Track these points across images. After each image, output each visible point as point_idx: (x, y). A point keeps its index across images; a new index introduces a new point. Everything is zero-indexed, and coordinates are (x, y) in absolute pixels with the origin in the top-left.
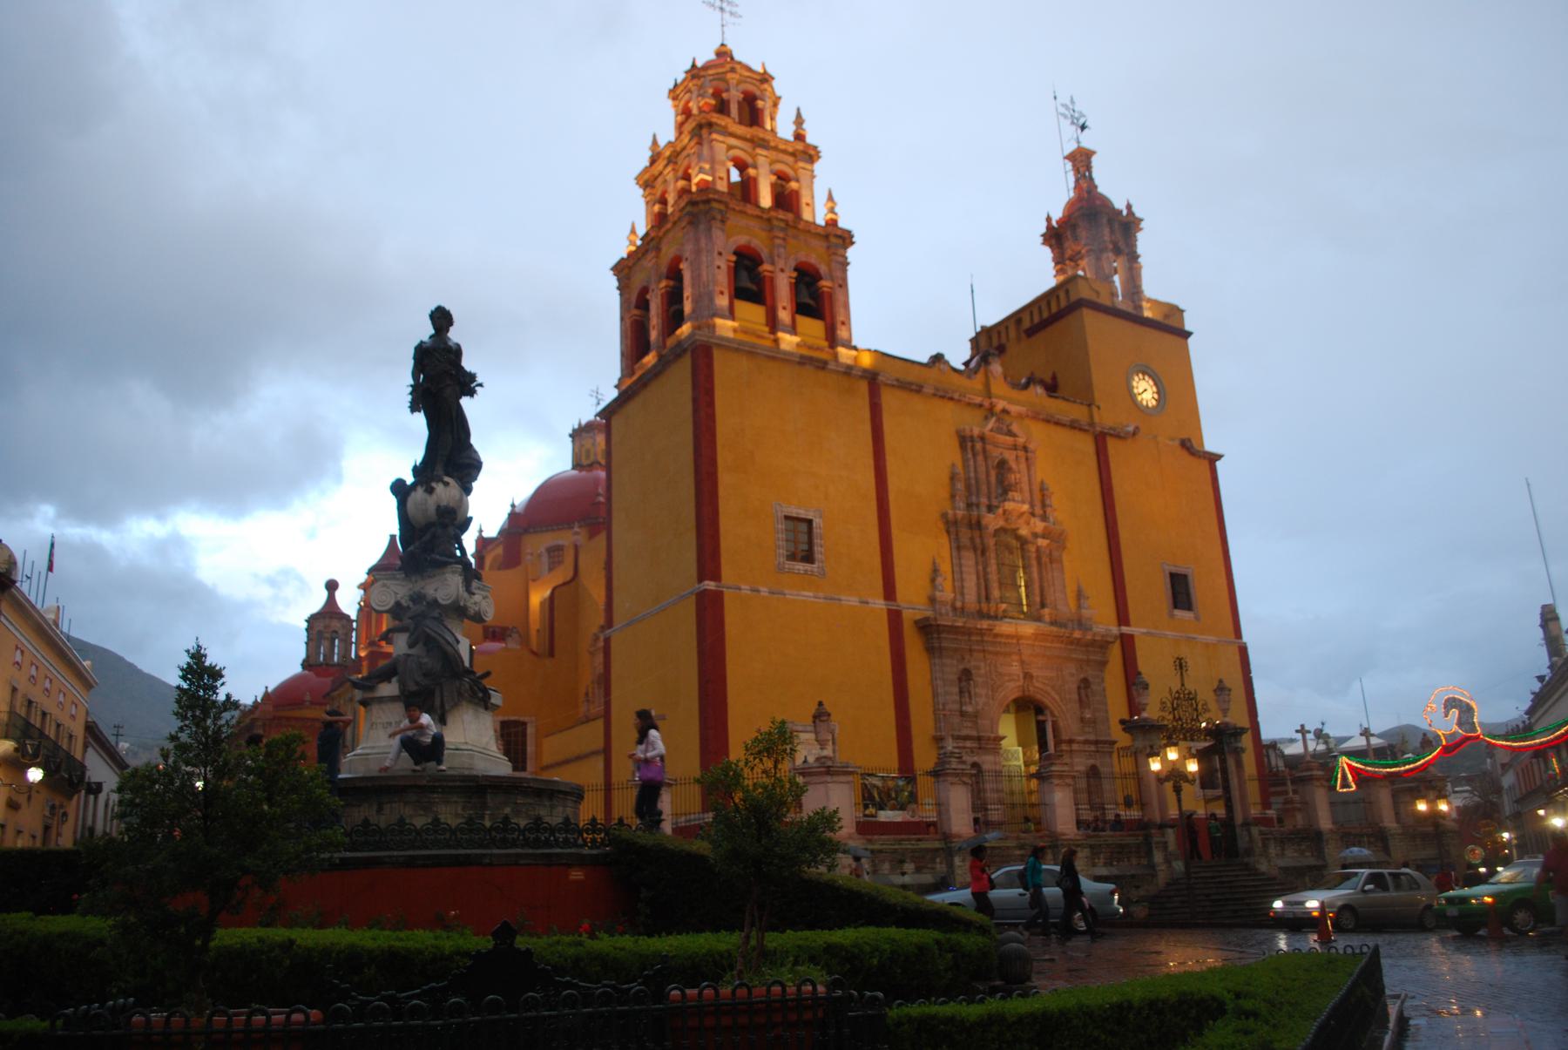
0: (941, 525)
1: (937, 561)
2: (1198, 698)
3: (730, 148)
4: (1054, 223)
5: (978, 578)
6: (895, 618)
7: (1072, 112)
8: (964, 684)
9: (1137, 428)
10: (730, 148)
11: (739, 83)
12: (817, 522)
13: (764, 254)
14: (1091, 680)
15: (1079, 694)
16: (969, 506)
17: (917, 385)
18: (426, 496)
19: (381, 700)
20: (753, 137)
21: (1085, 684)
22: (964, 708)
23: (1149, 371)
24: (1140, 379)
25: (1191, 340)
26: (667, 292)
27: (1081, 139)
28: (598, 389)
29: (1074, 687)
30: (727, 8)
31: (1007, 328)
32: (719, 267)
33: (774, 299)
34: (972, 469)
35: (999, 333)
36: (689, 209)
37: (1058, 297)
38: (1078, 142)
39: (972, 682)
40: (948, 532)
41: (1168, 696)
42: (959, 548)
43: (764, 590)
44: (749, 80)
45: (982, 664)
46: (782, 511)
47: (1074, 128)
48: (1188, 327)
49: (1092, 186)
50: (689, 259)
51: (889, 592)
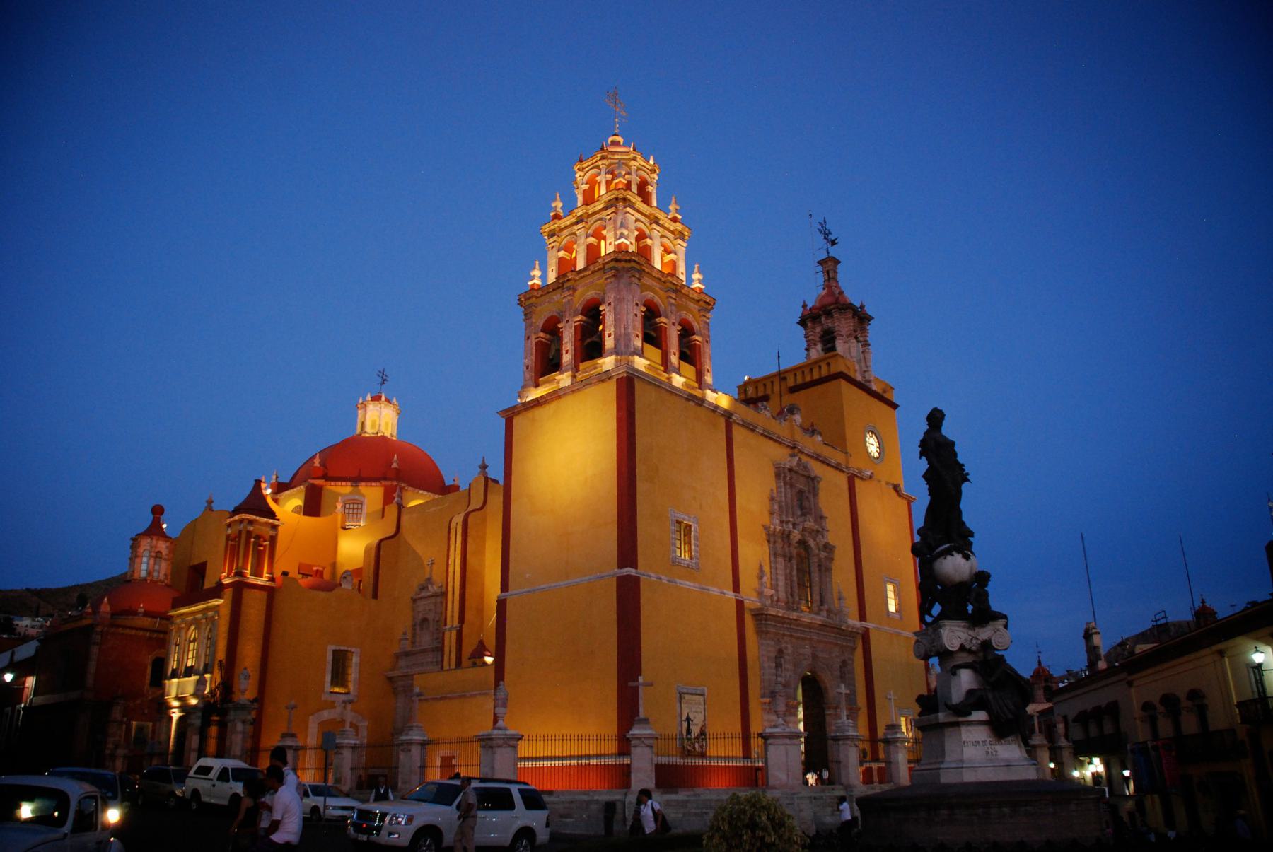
1: (763, 564)
3: (637, 220)
4: (808, 308)
5: (786, 579)
6: (740, 604)
9: (872, 473)
10: (637, 220)
11: (639, 169)
13: (662, 308)
16: (782, 522)
17: (754, 426)
18: (963, 561)
19: (970, 723)
20: (650, 214)
21: (844, 663)
23: (875, 431)
26: (582, 326)
27: (830, 251)
28: (384, 371)
29: (838, 666)
32: (636, 315)
34: (783, 495)
35: (765, 385)
36: (613, 264)
37: (820, 367)
38: (828, 253)
40: (769, 541)
42: (775, 555)
44: (643, 168)
45: (789, 646)
46: (675, 517)
47: (825, 241)
48: (895, 400)
50: (612, 304)
51: (736, 588)
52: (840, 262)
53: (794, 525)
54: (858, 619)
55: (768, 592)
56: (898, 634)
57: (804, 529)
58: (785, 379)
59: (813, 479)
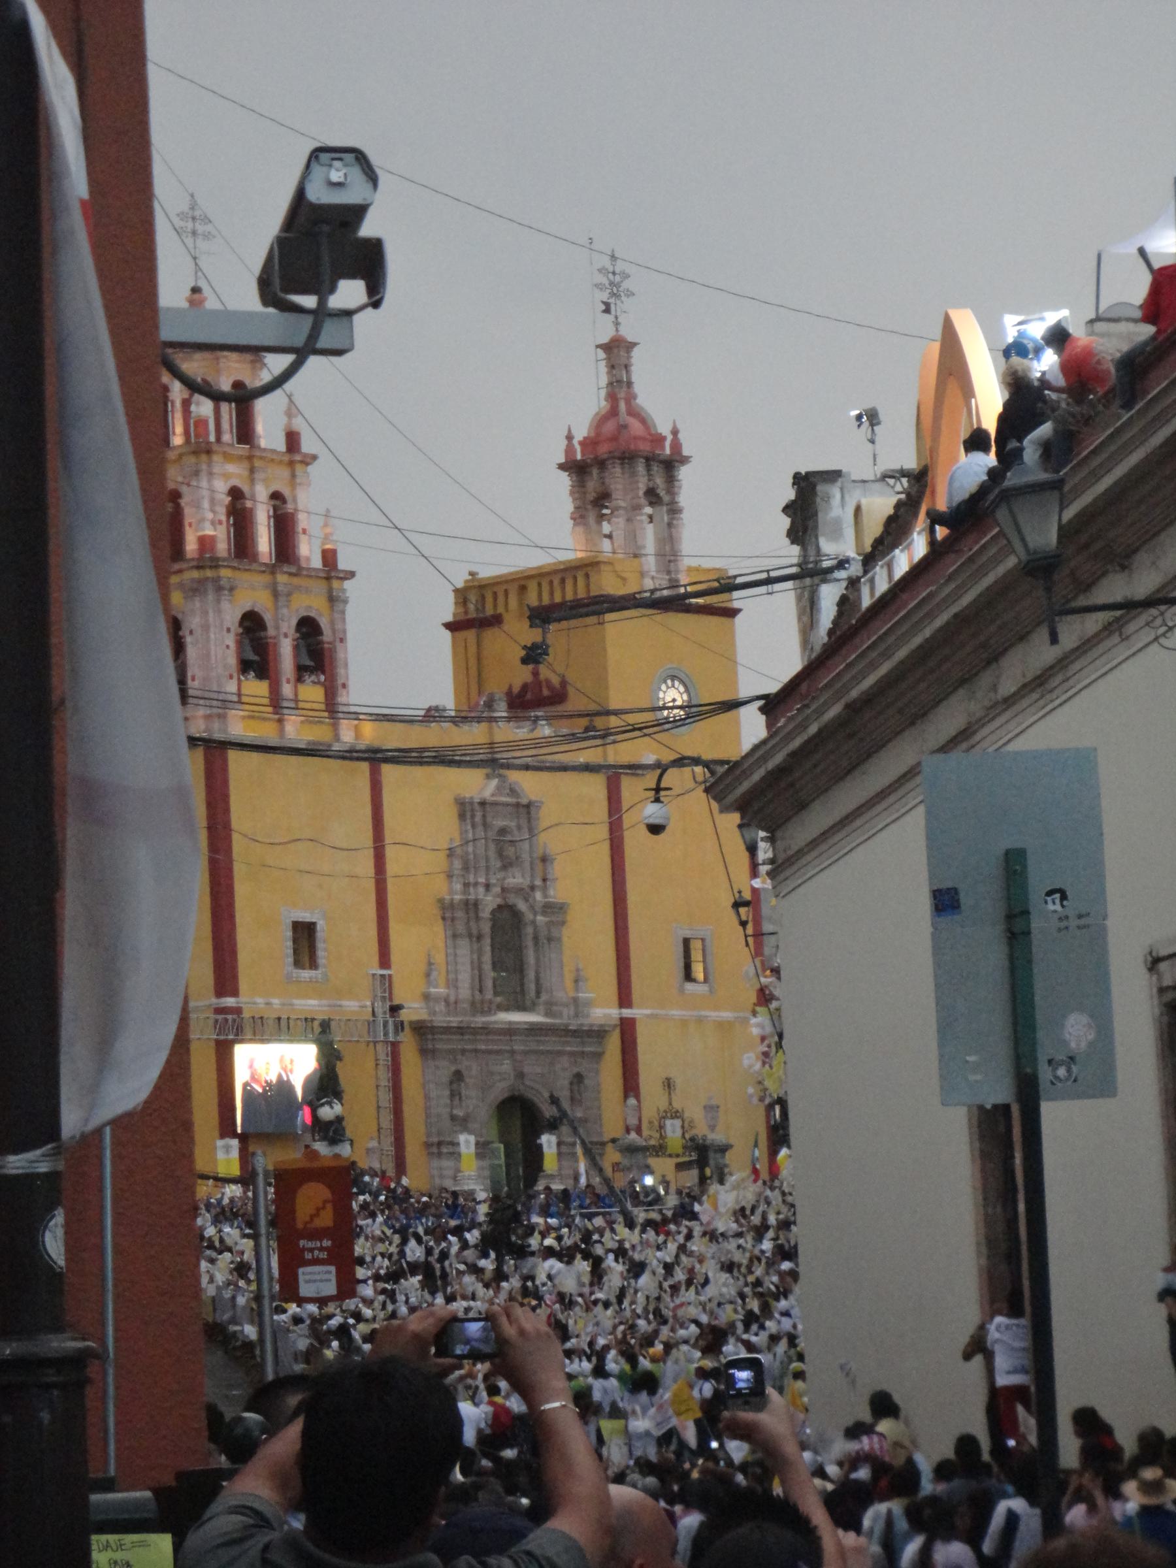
0: (436, 912)
2: (686, 1115)
5: (473, 969)
7: (611, 276)
8: (455, 1086)
12: (321, 925)
13: (268, 617)
14: (584, 1074)
15: (572, 1091)
16: (466, 885)
21: (579, 1077)
22: (455, 1112)
23: (682, 676)
24: (668, 687)
25: (739, 619)
29: (566, 1083)
30: (200, 228)
31: (506, 592)
32: (228, 647)
33: (278, 673)
37: (575, 578)
39: (463, 1084)
40: (444, 918)
41: (657, 1116)
42: (455, 936)
43: (276, 1001)
49: (631, 398)
52: (634, 344)
53: (488, 887)
54: (617, 1003)
55: (441, 990)
56: (700, 1020)
57: (503, 890)
58: (523, 589)
59: (528, 806)
